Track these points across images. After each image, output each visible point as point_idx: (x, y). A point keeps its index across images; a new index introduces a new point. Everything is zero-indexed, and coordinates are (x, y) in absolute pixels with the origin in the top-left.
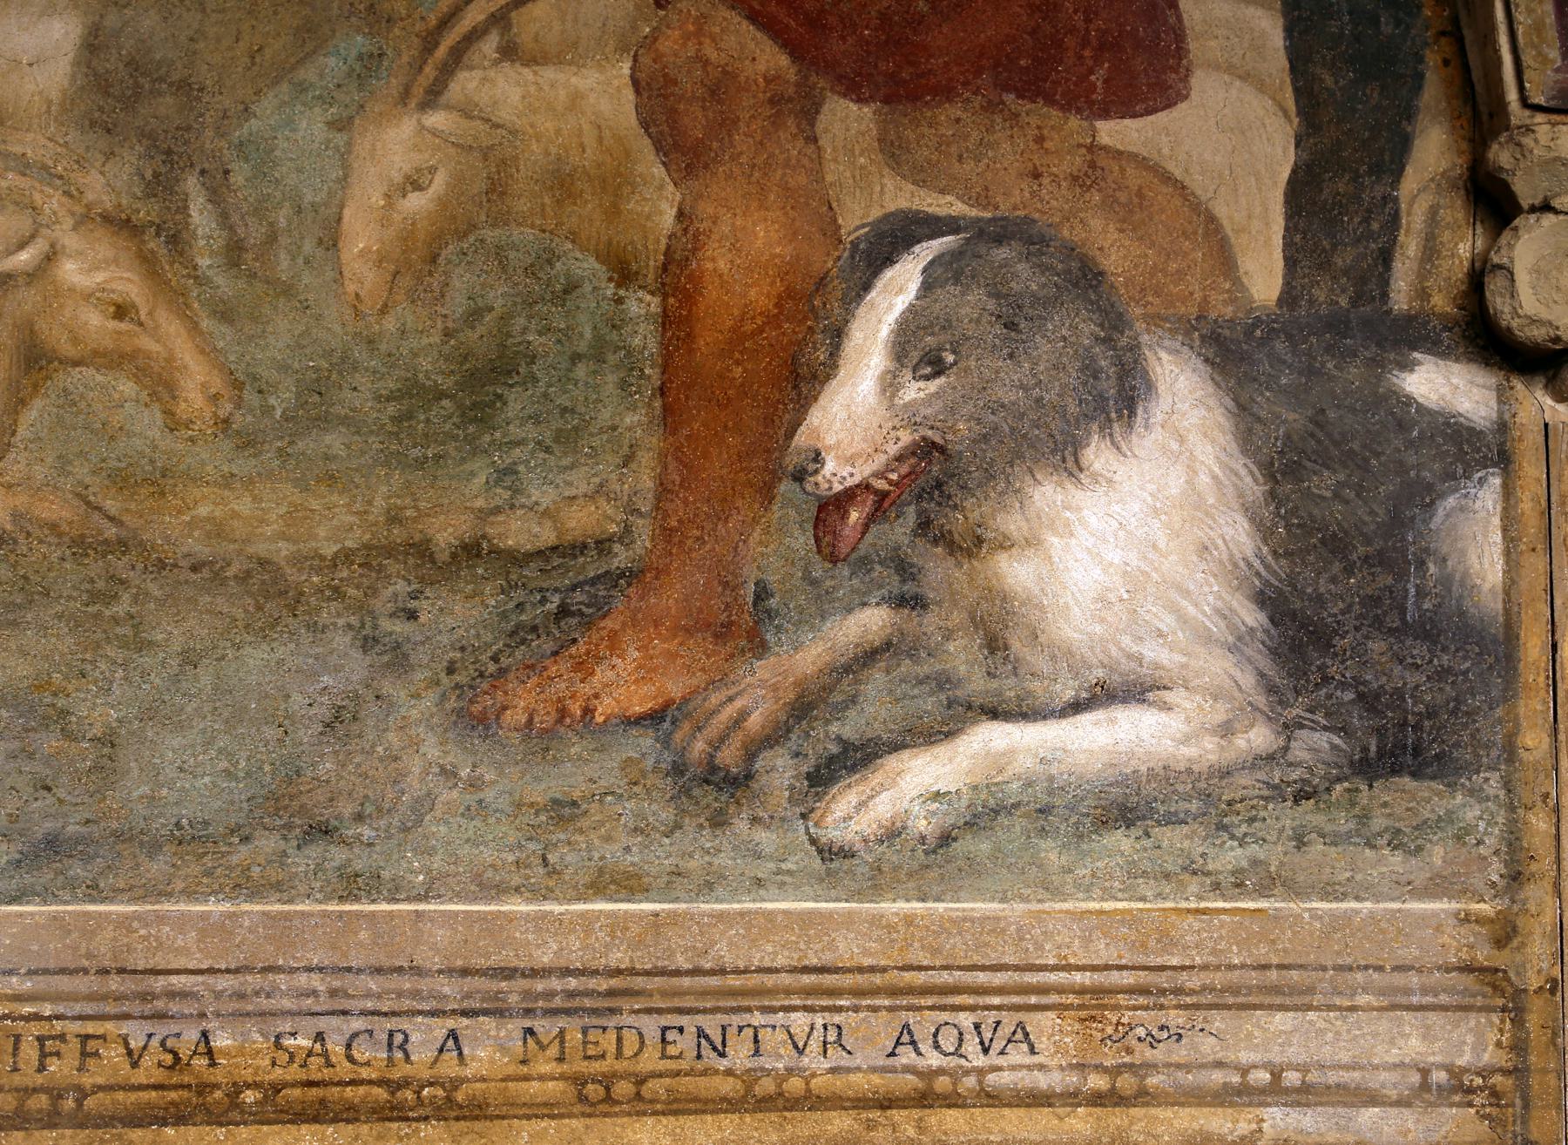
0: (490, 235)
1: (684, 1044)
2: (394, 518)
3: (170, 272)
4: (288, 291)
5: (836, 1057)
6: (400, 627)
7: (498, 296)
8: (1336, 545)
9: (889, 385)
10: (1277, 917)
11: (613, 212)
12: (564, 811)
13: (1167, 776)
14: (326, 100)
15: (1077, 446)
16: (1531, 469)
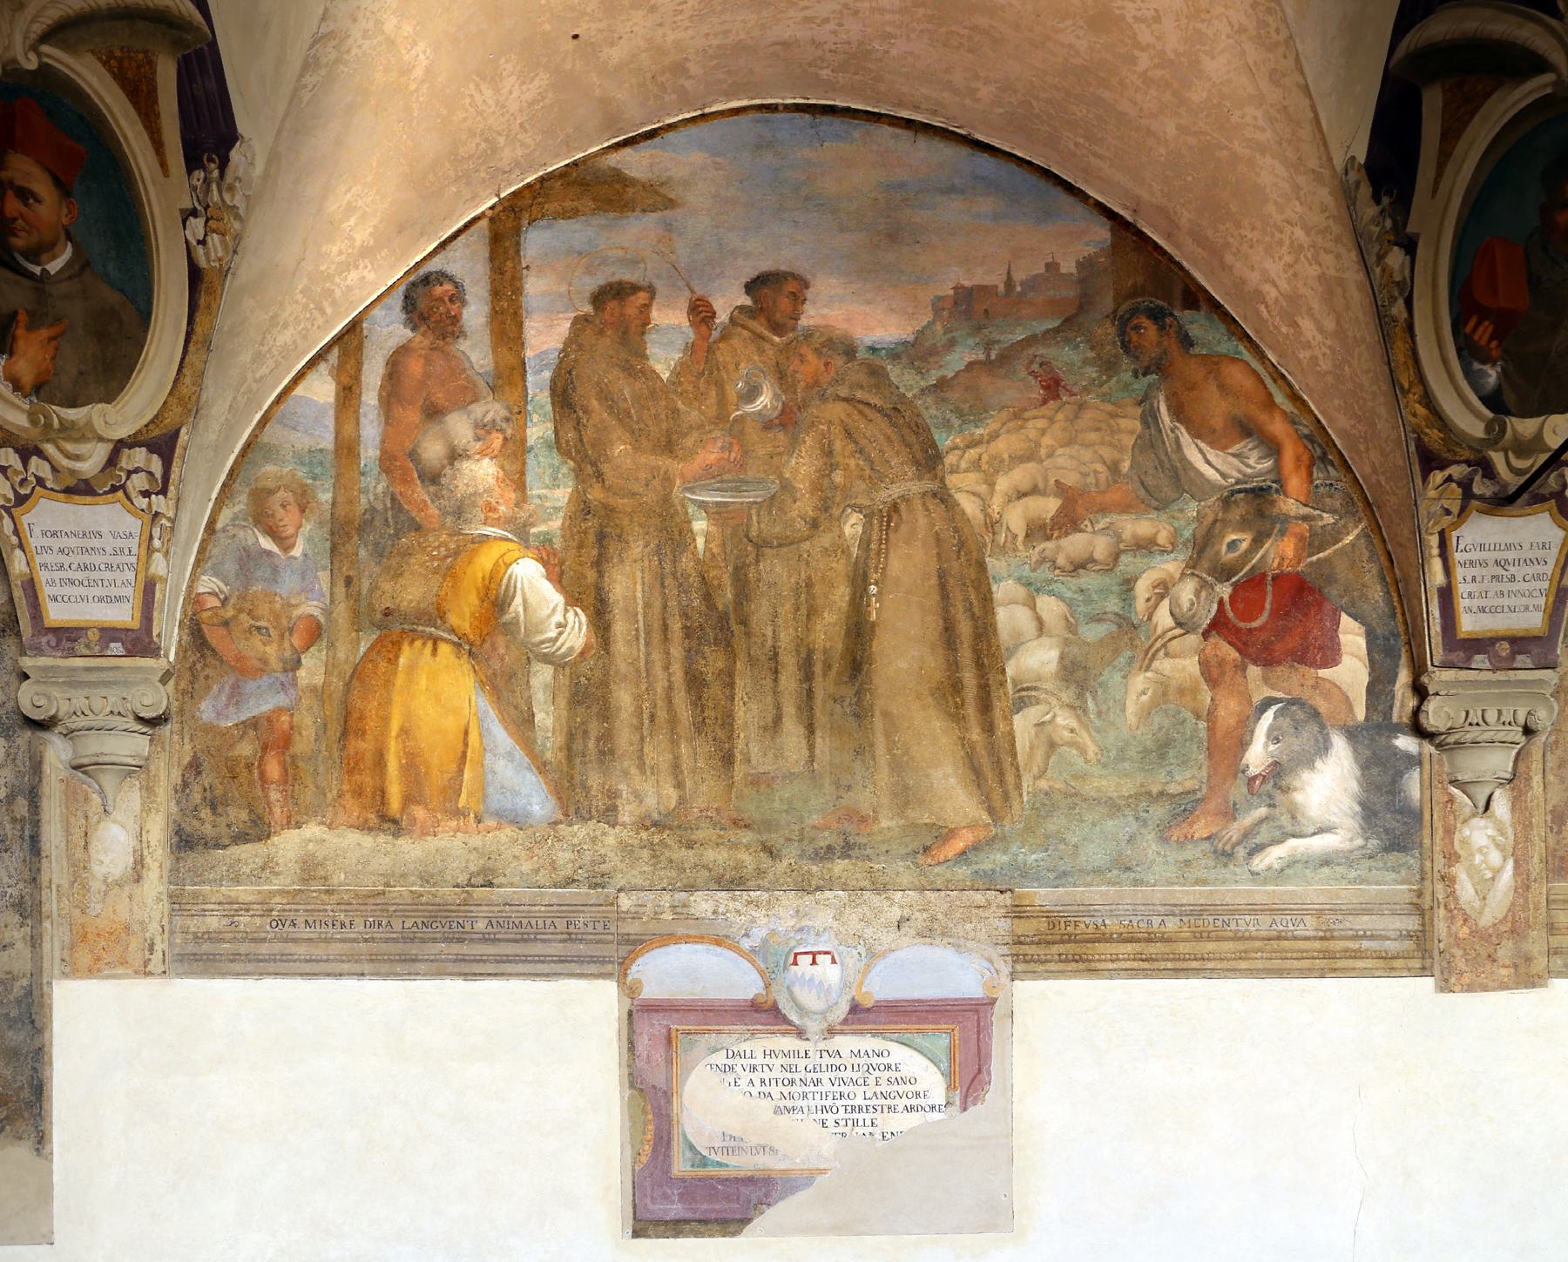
0: (1163, 707)
1: (1219, 923)
2: (1142, 786)
3: (1084, 719)
4: (1113, 724)
5: (1257, 927)
6: (1145, 815)
7: (1166, 723)
8: (1378, 788)
9: (1266, 746)
10: (1364, 890)
11: (1195, 699)
12: (1187, 863)
13: (1337, 852)
14: (1121, 670)
15: (1313, 762)
16: (1427, 766)
